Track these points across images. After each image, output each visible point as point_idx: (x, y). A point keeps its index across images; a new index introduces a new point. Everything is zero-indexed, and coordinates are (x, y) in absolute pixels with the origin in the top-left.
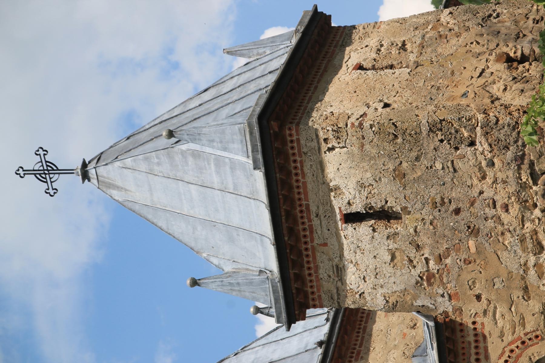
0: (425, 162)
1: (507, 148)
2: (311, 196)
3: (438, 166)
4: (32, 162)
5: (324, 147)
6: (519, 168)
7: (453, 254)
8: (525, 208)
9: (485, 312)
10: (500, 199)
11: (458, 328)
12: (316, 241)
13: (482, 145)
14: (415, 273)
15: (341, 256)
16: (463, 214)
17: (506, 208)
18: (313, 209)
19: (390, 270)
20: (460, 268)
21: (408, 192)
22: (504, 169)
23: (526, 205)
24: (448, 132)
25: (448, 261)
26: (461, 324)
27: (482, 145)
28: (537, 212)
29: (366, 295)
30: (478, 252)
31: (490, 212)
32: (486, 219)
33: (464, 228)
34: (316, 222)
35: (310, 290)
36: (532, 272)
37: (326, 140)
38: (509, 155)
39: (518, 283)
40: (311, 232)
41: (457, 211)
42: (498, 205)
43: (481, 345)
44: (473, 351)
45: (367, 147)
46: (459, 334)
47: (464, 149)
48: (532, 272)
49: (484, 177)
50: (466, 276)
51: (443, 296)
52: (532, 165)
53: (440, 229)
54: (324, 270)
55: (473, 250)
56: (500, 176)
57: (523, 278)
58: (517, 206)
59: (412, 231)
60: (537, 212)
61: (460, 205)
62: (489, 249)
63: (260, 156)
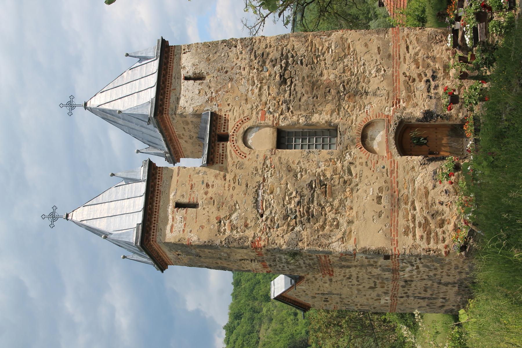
0: (218, 54)
1: (247, 47)
2: (174, 70)
3: (223, 55)
4: (66, 110)
5: (183, 52)
6: (251, 54)
7: (222, 90)
8: (251, 69)
9: (230, 110)
10: (242, 66)
11: (219, 117)
12: (172, 88)
13: (239, 46)
14: (207, 97)
15: (180, 93)
16: (228, 73)
17: (244, 69)
18: (174, 75)
19: (198, 97)
20: (224, 94)
21: (210, 66)
22: (245, 55)
23: (251, 67)
24: (229, 44)
25: (220, 93)
26: (220, 116)
27: (239, 46)
28: (255, 70)
29: (186, 108)
30: (231, 87)
31: (238, 71)
32: (236, 74)
33: (227, 78)
34: (173, 80)
35: (165, 107)
36: (250, 92)
37: (184, 50)
38: (248, 49)
39: (244, 98)
40: (171, 84)
41: (226, 72)
42: (241, 68)
43: (226, 124)
44: (223, 127)
45: (199, 50)
46: (219, 120)
47: (233, 48)
48: (250, 92)
49: (238, 58)
50: (225, 97)
51: (215, 105)
52: (255, 53)
53: (219, 80)
54: (173, 99)
55: (230, 87)
56: (244, 57)
57: (246, 95)
58: (248, 68)
59: (209, 81)
60: (255, 70)
61: (228, 69)
62: (236, 86)
63: (159, 51)
